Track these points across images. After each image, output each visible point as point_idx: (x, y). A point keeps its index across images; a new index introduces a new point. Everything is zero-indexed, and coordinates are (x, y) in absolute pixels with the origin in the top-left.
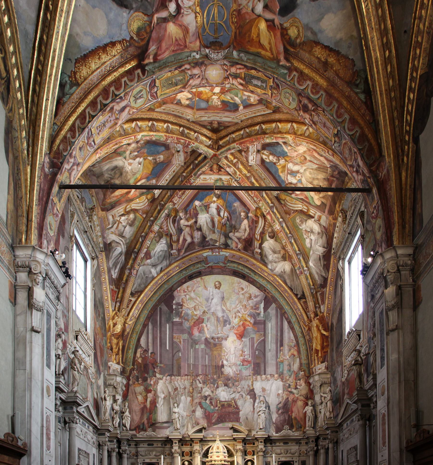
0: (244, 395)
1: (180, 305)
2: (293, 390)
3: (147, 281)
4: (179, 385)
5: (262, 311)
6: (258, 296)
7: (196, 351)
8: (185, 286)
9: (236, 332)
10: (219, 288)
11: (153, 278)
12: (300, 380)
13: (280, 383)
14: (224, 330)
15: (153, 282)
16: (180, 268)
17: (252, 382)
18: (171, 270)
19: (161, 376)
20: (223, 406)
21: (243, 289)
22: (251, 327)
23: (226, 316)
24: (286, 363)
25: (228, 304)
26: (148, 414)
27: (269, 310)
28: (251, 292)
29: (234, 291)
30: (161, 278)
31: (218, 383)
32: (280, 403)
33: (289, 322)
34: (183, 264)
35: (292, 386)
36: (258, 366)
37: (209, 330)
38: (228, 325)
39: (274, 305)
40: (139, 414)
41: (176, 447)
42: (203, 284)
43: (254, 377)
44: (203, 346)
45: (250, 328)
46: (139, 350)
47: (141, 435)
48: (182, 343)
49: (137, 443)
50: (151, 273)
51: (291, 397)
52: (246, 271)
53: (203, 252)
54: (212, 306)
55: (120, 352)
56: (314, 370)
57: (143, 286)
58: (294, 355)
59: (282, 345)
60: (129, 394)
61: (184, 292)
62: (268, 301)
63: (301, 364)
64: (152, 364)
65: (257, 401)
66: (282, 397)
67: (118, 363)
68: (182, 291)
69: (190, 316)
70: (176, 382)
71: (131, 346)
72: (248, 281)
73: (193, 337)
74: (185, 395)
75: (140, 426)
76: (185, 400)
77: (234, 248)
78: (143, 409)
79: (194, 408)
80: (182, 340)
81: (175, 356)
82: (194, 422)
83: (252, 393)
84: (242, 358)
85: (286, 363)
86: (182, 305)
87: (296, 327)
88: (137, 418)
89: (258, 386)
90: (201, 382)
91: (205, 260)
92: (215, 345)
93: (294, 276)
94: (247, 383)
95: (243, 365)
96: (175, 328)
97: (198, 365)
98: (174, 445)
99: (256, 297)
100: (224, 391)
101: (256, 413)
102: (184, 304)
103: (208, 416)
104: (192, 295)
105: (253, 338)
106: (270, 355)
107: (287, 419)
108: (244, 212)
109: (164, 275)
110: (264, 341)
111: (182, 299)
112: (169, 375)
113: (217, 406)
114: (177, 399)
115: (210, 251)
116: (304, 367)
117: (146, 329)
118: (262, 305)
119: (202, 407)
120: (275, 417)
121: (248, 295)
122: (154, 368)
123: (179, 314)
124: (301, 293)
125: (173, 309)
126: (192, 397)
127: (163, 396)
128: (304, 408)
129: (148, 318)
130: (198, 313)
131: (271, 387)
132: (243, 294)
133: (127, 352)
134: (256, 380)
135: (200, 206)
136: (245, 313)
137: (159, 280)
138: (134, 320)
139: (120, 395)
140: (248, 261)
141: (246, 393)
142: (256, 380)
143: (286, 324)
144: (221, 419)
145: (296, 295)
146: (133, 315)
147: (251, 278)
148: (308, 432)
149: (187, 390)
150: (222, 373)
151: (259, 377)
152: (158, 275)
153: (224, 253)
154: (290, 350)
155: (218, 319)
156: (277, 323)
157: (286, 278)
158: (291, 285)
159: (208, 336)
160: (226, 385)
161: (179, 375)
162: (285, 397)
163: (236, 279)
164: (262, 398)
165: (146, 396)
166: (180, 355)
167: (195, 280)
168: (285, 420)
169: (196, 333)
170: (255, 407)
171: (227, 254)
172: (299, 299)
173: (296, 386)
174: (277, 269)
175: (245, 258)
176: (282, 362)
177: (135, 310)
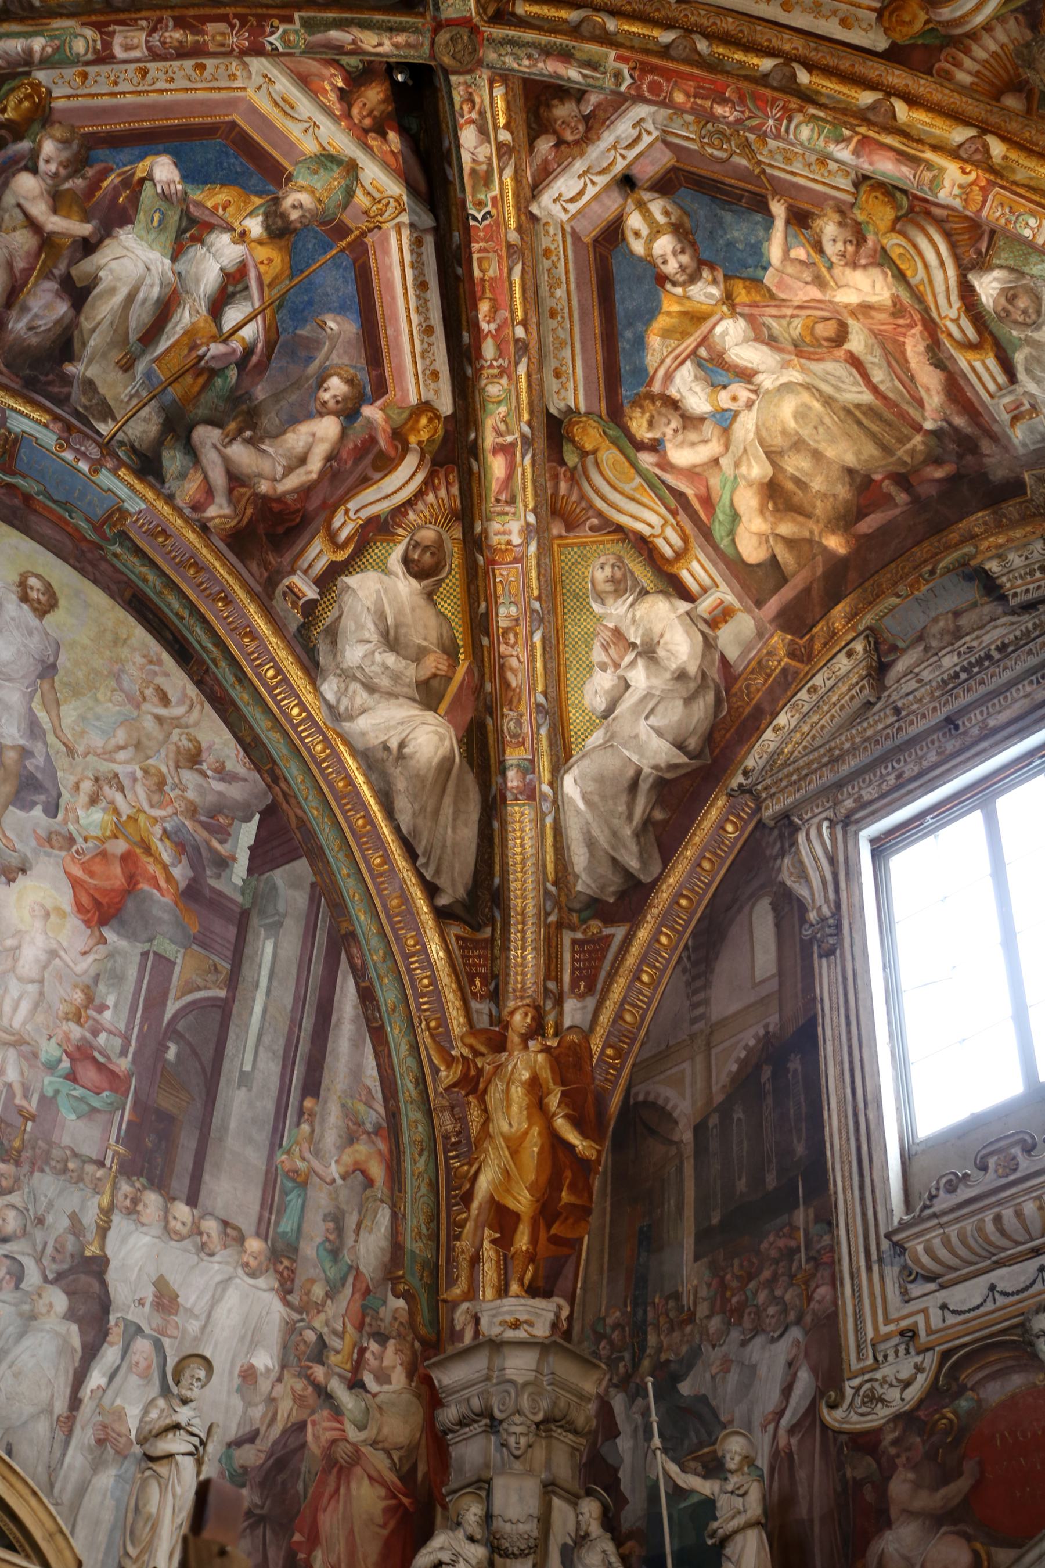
0: (33, 1277)
2: (337, 1387)
9: (78, 872)
17: (107, 1212)
21: (164, 699)
22: (167, 900)
23: (40, 760)
24: (320, 1199)
25: (70, 713)
27: (279, 876)
29: (118, 679)
32: (252, 1438)
35: (333, 1359)
38: (37, 812)
43: (125, 1188)
58: (370, 1182)
63: (396, 1247)
65: (110, 1355)
66: (271, 1400)
72: (199, 684)
77: (179, 502)
84: (76, 1032)
85: (320, 1199)
93: (448, 800)
95: (72, 1077)
99: (222, 773)
110: (222, 1014)
115: (57, 427)
116: (414, 1279)
118: (247, 833)
121: (185, 743)
124: (461, 892)
132: (159, 719)
134: (133, 1211)
140: (227, 600)
142: (133, 1211)
145: (431, 890)
151: (152, 1199)
153: (123, 492)
154: (351, 1139)
156: (305, 963)
157: (401, 785)
158: (415, 831)
163: (140, 634)
170: (86, 1393)
171: (134, 506)
172: (442, 915)
173: (358, 1365)
174: (363, 723)
175: (214, 577)
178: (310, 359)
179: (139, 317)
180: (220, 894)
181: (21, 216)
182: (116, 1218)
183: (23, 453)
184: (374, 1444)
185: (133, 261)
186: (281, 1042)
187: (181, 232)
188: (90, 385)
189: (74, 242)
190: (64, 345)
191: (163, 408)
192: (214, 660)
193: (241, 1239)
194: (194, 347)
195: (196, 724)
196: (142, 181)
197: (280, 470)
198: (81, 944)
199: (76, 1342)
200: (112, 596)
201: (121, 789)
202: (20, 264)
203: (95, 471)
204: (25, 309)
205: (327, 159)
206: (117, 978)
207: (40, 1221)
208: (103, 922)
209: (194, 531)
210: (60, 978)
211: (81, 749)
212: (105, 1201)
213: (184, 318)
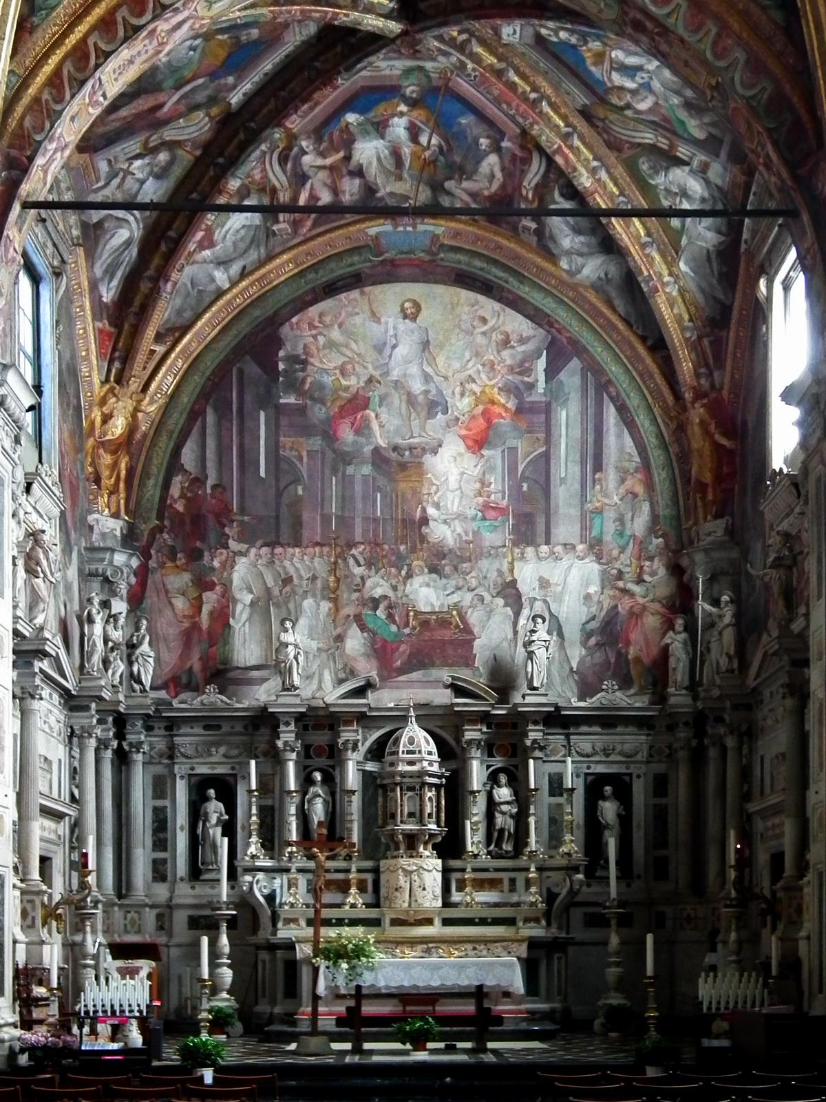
0: (488, 598)
1: (300, 362)
3: (199, 301)
4: (297, 570)
5: (542, 378)
6: (528, 339)
7: (347, 482)
8: (313, 311)
9: (464, 432)
10: (414, 318)
11: (220, 294)
12: (651, 559)
13: (592, 568)
14: (428, 427)
15: (220, 303)
16: (297, 265)
18: (271, 272)
19: (243, 547)
20: (425, 624)
21: (484, 320)
22: (508, 421)
23: (434, 392)
24: (610, 515)
25: (441, 360)
26: (205, 645)
27: (562, 376)
28: (508, 328)
29: (459, 326)
31: (409, 565)
32: (593, 618)
33: (622, 409)
34: (308, 254)
35: (627, 576)
36: (528, 521)
37: (385, 426)
39: (575, 363)
40: (176, 646)
41: (288, 735)
42: (366, 308)
43: (517, 550)
44: (367, 469)
45: (504, 422)
46: (177, 480)
47: (186, 703)
48: (305, 460)
49: (172, 725)
51: (624, 606)
52: (495, 274)
53: (368, 224)
54: (392, 363)
55: (122, 485)
56: (693, 533)
57: (188, 314)
58: (635, 495)
59: (598, 466)
60: (148, 593)
61: (311, 326)
62: (559, 352)
63: (655, 518)
64: (217, 516)
65: (526, 612)
66: (599, 602)
67: (116, 515)
68: (306, 326)
69: (327, 391)
70: (287, 563)
71: (154, 469)
72: (500, 300)
73: (336, 446)
74: (314, 596)
75: (179, 678)
76: (313, 609)
78: (190, 635)
79: (339, 630)
80: (305, 454)
81: (285, 495)
82: (340, 666)
83: (510, 593)
84: (481, 500)
85: (610, 515)
86: (305, 363)
87: (643, 420)
88: (171, 658)
89: (527, 574)
90: (362, 562)
91: (374, 246)
92: (403, 466)
94: (496, 565)
95: (484, 519)
96: (284, 421)
97: (353, 518)
98: (282, 728)
99: (522, 341)
100: (428, 585)
101: (520, 643)
102: (312, 360)
103: (381, 651)
104: (335, 334)
105: (513, 450)
106: (564, 494)
107: (613, 660)
108: (488, 137)
109: (252, 284)
110: (546, 457)
111: (305, 346)
112: (266, 545)
113: (407, 625)
114: (291, 606)
117: (198, 423)
118: (541, 363)
119: (363, 628)
120: (576, 654)
121: (501, 337)
122: (223, 526)
123: (295, 386)
125: (278, 373)
126: (335, 601)
127: (248, 598)
128: (664, 635)
129: (204, 396)
130: (352, 382)
131: (566, 577)
132: (484, 333)
133: (142, 485)
135: (360, 124)
136: (490, 384)
138: (162, 401)
139: (121, 598)
140: (499, 247)
141: (494, 592)
143: (611, 413)
144: (420, 660)
146: (159, 387)
147: (510, 291)
148: (672, 700)
149: (319, 584)
150: (423, 539)
151: (530, 550)
152: (234, 284)
153: (431, 228)
154: (623, 481)
155: (411, 400)
159: (382, 443)
160: (433, 569)
161: (297, 543)
162: (607, 604)
163: (465, 295)
164: (539, 607)
165: (200, 598)
166: (300, 492)
167: (343, 296)
168: (606, 664)
169: (347, 434)
171: (439, 231)
176: (599, 512)
177: (165, 377)
178: (466, 137)
179: (389, 164)
180: (533, 402)
182: (516, 564)
183: (383, 241)
184: (652, 601)
185: (368, 151)
186: (578, 455)
187: (377, 130)
188: (391, 194)
190: (370, 190)
191: (426, 184)
192: (507, 282)
193: (574, 547)
194: (419, 158)
195: (503, 323)
197: (487, 184)
198: (473, 464)
199: (511, 613)
200: (446, 284)
201: (474, 381)
202: (329, 181)
203: (414, 226)
204: (344, 192)
205: (408, 72)
206: (492, 469)
207: (485, 577)
208: (480, 448)
209: (470, 225)
210: (468, 482)
211: (450, 374)
212: (510, 559)
213: (407, 151)
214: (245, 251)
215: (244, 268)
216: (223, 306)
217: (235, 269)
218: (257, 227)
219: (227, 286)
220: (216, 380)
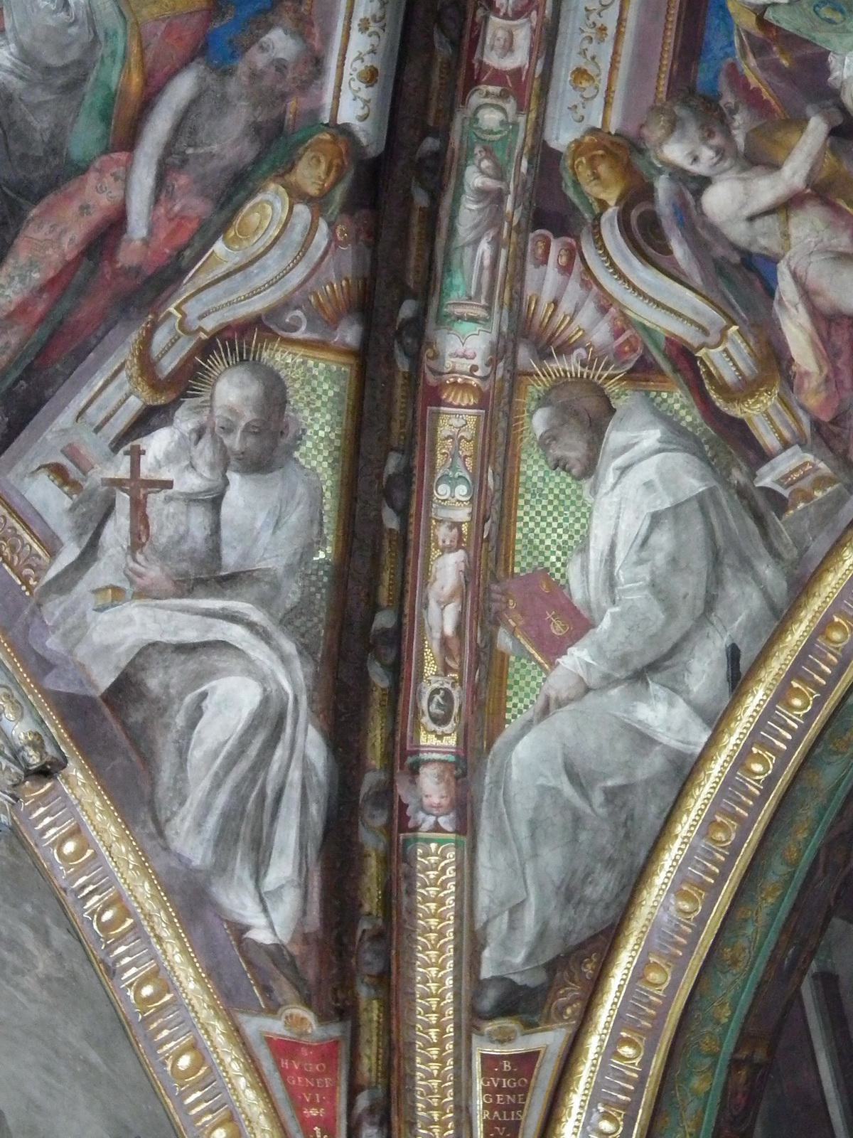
3: (626, 826)
11: (685, 771)
18: (824, 626)
30: (754, 737)
50: (643, 739)
109: (782, 694)
137: (742, 759)
152: (718, 722)
181: (769, 221)
189: (832, 149)
196: (762, 23)
214: (710, 603)
215: (733, 654)
216: (716, 805)
217: (703, 671)
218: (703, 502)
219: (704, 738)
220: (760, 1055)
